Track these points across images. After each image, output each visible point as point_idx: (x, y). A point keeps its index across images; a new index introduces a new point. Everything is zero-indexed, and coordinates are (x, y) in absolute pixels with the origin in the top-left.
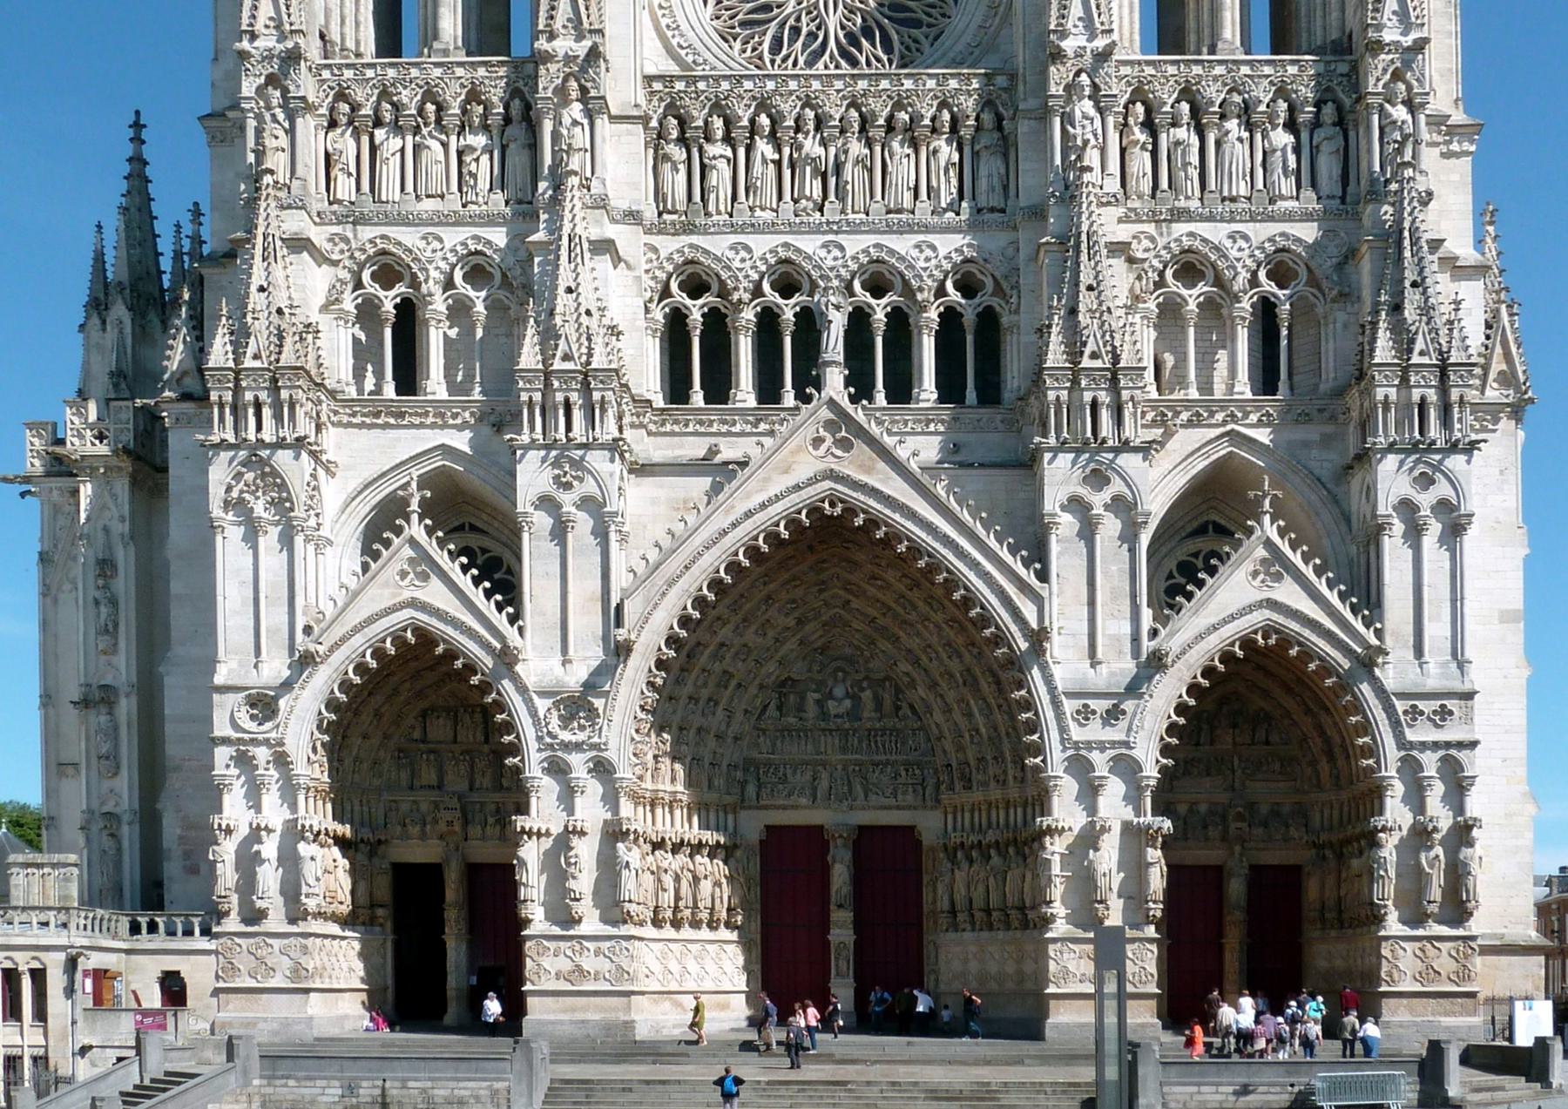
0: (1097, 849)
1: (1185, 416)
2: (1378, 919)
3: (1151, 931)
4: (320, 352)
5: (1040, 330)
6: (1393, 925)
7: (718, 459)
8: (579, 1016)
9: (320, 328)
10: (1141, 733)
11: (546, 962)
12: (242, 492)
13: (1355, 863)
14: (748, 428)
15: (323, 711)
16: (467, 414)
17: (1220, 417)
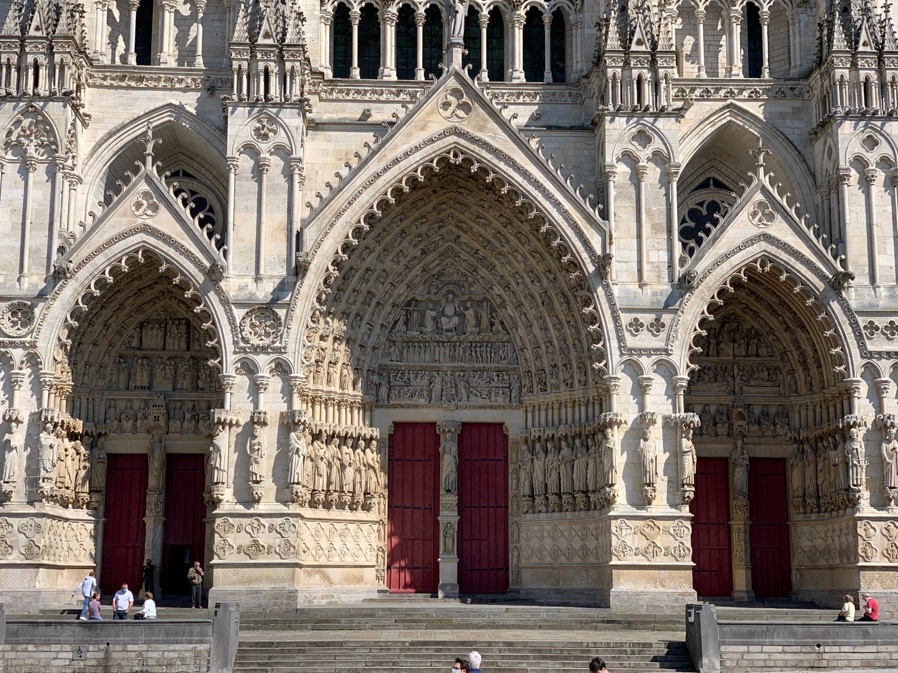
0: (646, 440)
1: (698, 92)
2: (853, 502)
3: (686, 511)
4: (84, 28)
5: (598, 24)
6: (866, 509)
7: (370, 120)
8: (255, 586)
9: (85, 9)
10: (676, 342)
11: (231, 538)
12: (19, 136)
13: (832, 453)
14: (392, 97)
15: (69, 318)
16: (189, 81)
17: (722, 93)
